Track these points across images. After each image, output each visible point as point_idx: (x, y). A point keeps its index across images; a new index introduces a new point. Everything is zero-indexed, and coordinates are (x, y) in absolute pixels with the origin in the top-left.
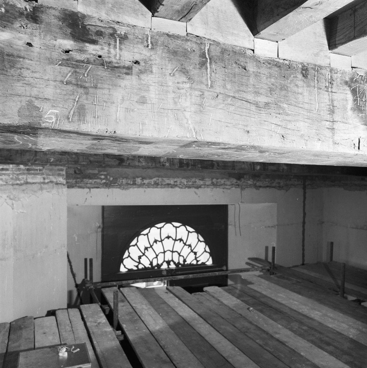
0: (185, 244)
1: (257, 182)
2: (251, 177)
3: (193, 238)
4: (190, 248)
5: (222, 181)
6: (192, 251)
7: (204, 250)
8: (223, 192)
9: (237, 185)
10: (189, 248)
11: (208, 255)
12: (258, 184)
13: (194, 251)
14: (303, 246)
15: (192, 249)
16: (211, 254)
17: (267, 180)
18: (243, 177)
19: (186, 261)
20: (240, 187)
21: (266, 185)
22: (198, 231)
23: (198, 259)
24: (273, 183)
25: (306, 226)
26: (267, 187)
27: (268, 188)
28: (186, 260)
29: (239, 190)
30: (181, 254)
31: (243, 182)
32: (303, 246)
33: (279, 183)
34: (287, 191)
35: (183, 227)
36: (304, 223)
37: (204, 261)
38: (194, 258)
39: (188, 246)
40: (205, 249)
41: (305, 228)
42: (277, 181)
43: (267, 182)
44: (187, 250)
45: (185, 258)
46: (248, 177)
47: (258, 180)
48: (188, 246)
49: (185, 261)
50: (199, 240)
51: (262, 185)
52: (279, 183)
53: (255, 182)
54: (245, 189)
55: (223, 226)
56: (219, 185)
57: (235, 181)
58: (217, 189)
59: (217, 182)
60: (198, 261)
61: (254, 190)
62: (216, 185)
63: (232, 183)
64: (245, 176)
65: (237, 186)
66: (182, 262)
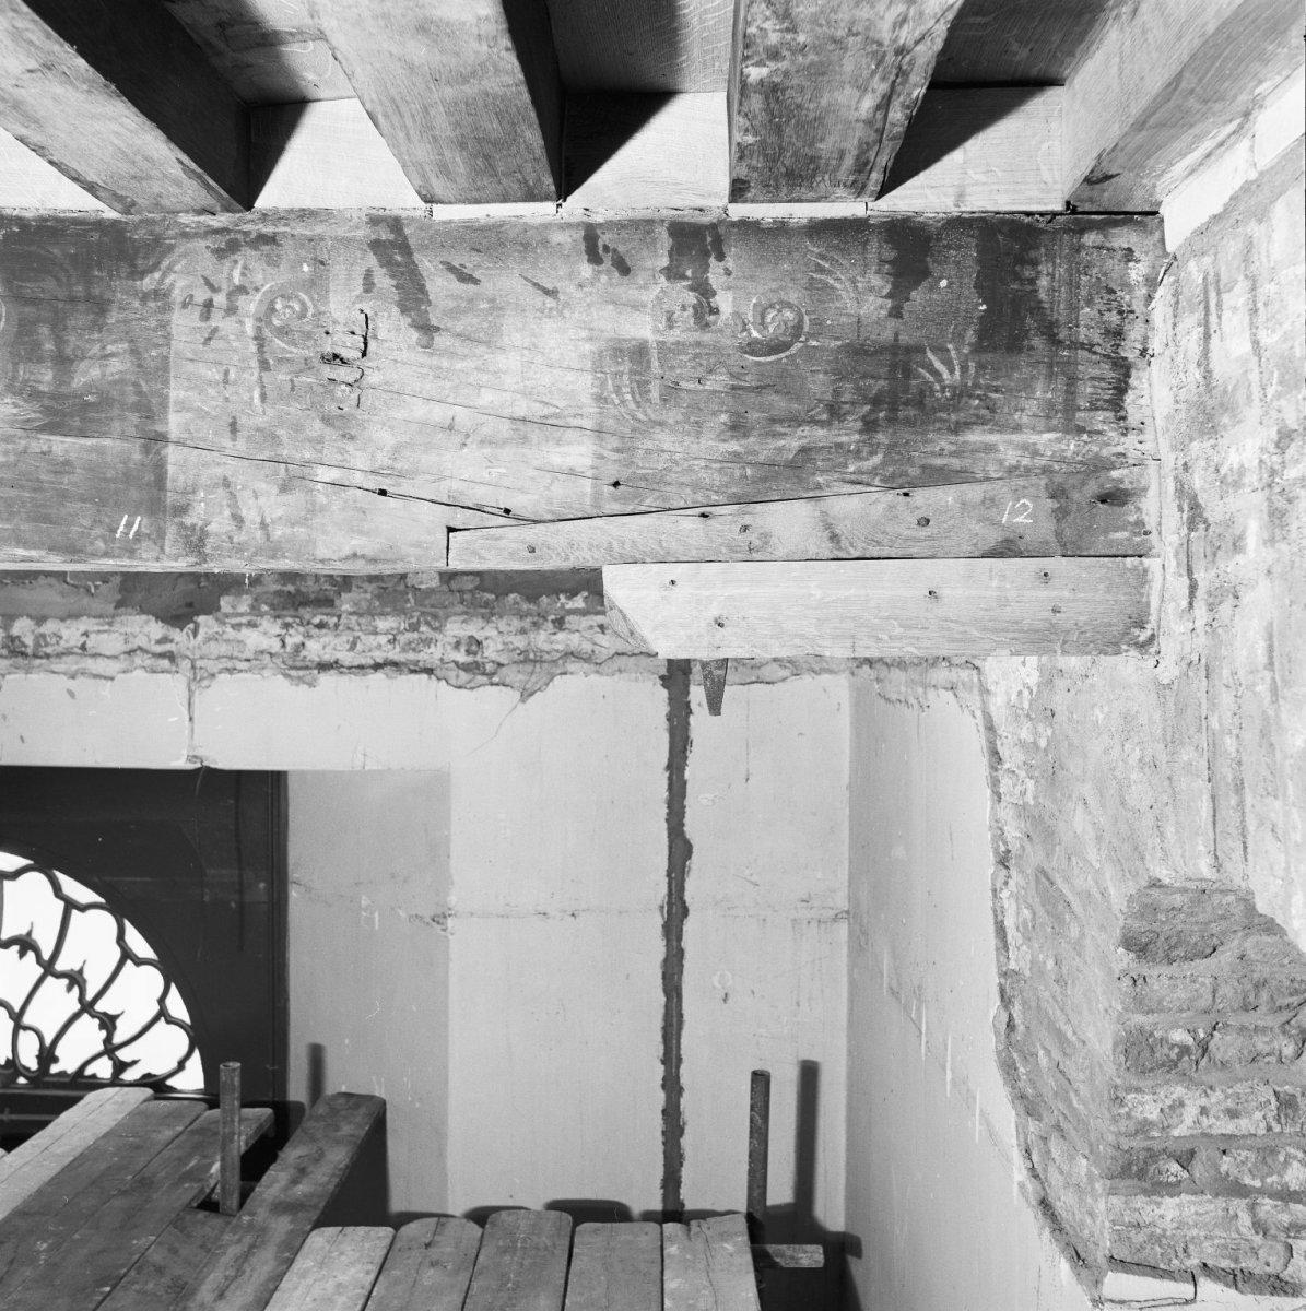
0: (48, 968)
1: (309, 636)
2: (265, 608)
3: (95, 937)
4: (76, 990)
5: (71, 633)
6: (87, 1007)
7: (157, 1008)
8: (71, 694)
9: (162, 656)
10: (69, 989)
11: (181, 1041)
12: (316, 649)
13: (100, 1007)
14: (672, 1058)
15: (89, 996)
16: (199, 1036)
17: (383, 624)
18: (211, 608)
19: (56, 1060)
20: (186, 664)
21: (379, 657)
22: (119, 906)
23: (124, 1055)
24: (428, 642)
25: (689, 927)
26: (377, 667)
27: (380, 675)
28: (58, 1052)
29: (174, 685)
30: (27, 1020)
31: (209, 639)
32: (672, 1058)
33: (475, 644)
34: (526, 694)
35: (37, 880)
36: (676, 913)
37: (159, 1069)
38: (101, 1047)
39: (65, 982)
40: (162, 1000)
41: (689, 941)
42: (456, 628)
43: (383, 639)
44: (55, 1003)
45: (48, 1042)
46: (243, 607)
47: (321, 626)
48: (65, 982)
49: (47, 1055)
50: (127, 955)
51: (347, 658)
52: (475, 644)
53: (294, 638)
54: (213, 676)
55: (262, 885)
56: (48, 656)
57: (156, 629)
58: (33, 677)
59: (41, 639)
60: (120, 1067)
61: (276, 686)
62: (35, 656)
63: (141, 641)
64: (225, 603)
65: (165, 663)
66: (29, 1060)
